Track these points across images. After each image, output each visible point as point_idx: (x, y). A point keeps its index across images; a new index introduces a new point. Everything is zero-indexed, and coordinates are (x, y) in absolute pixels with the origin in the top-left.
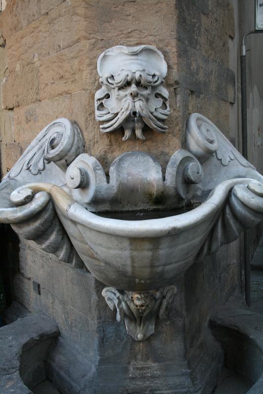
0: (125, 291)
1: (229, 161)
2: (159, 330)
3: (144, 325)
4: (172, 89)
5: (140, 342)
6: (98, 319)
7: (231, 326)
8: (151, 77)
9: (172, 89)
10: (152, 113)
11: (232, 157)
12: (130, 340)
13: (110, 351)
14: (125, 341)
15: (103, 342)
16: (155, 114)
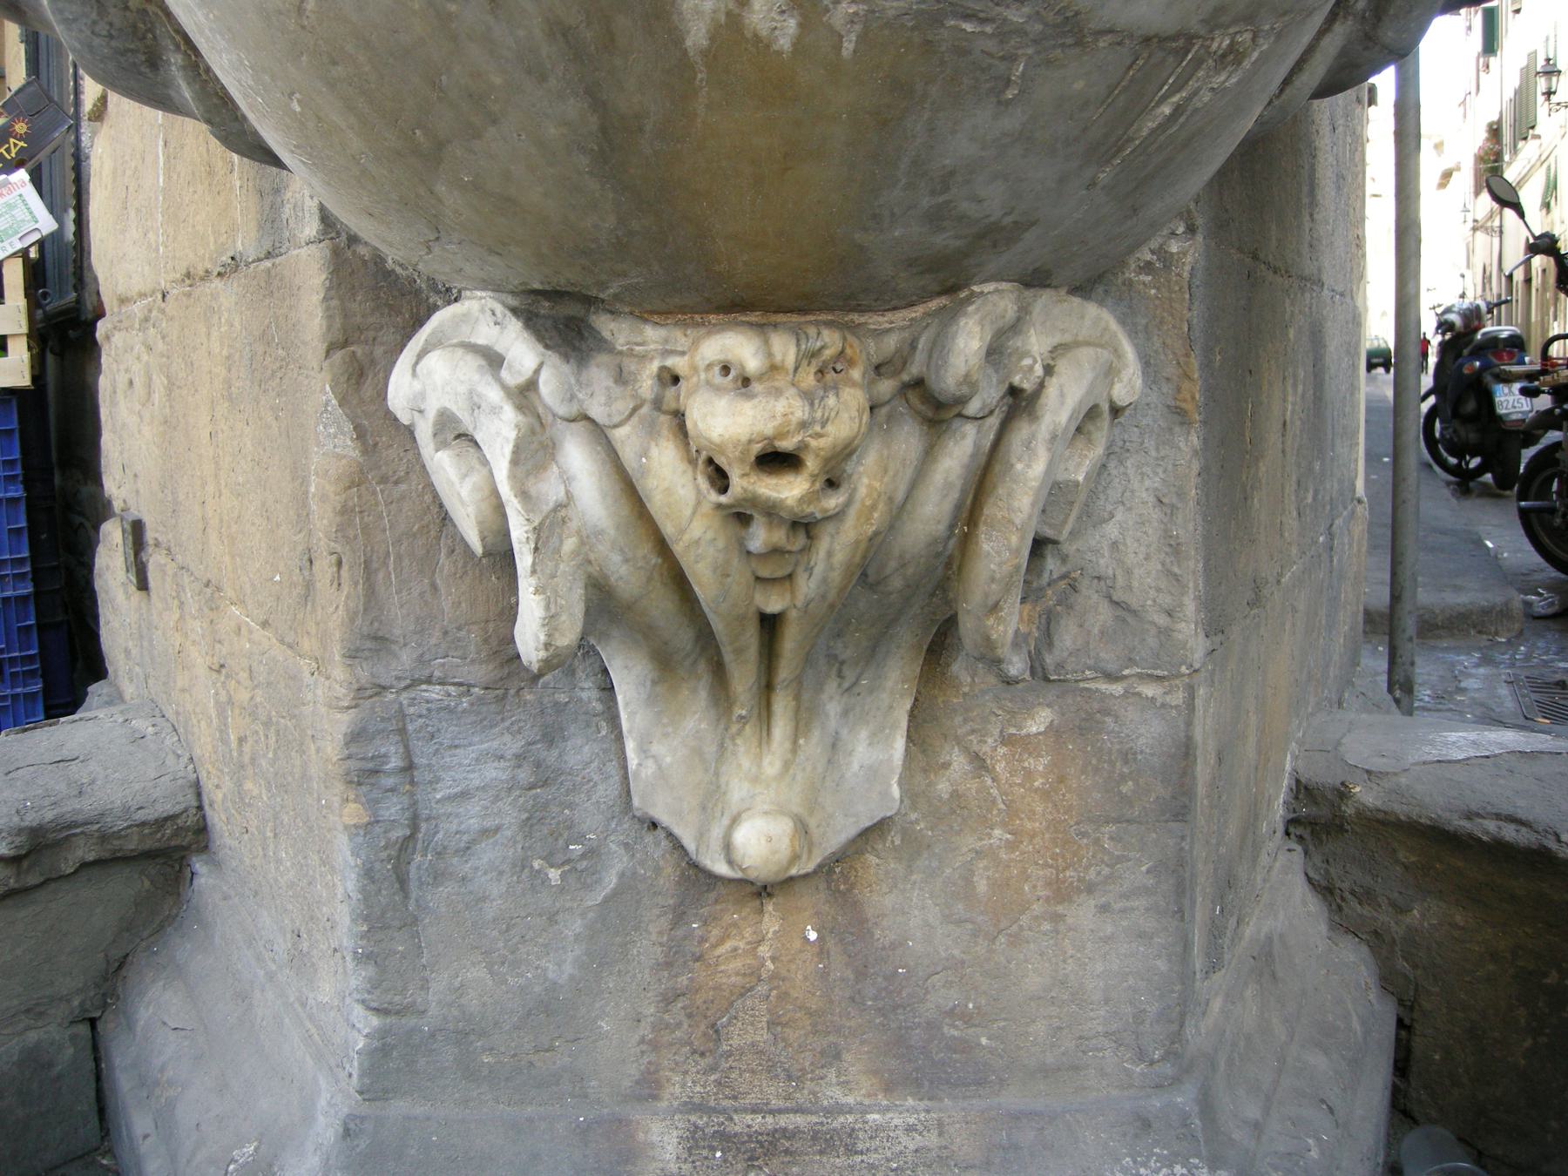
0: (607, 326)
2: (943, 787)
3: (802, 723)
5: (760, 891)
6: (352, 655)
7: (1470, 815)
12: (670, 872)
13: (476, 973)
14: (611, 880)
15: (403, 882)
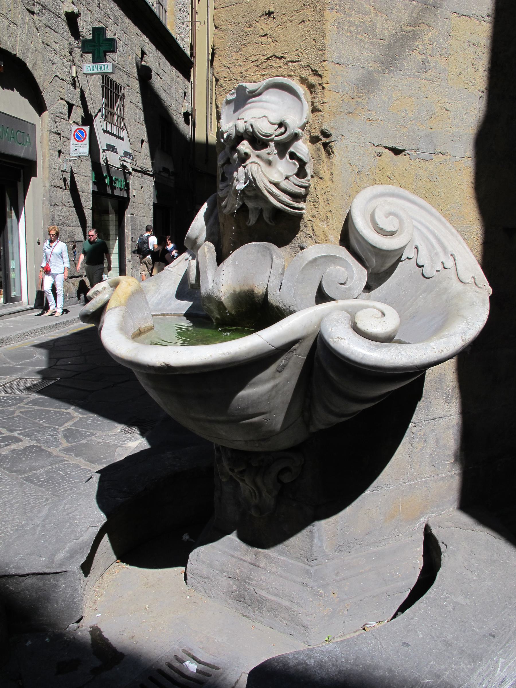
1: (438, 271)
4: (319, 145)
8: (277, 126)
9: (319, 145)
10: (276, 185)
11: (449, 264)
16: (284, 184)
